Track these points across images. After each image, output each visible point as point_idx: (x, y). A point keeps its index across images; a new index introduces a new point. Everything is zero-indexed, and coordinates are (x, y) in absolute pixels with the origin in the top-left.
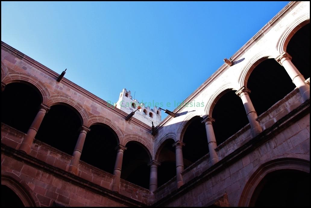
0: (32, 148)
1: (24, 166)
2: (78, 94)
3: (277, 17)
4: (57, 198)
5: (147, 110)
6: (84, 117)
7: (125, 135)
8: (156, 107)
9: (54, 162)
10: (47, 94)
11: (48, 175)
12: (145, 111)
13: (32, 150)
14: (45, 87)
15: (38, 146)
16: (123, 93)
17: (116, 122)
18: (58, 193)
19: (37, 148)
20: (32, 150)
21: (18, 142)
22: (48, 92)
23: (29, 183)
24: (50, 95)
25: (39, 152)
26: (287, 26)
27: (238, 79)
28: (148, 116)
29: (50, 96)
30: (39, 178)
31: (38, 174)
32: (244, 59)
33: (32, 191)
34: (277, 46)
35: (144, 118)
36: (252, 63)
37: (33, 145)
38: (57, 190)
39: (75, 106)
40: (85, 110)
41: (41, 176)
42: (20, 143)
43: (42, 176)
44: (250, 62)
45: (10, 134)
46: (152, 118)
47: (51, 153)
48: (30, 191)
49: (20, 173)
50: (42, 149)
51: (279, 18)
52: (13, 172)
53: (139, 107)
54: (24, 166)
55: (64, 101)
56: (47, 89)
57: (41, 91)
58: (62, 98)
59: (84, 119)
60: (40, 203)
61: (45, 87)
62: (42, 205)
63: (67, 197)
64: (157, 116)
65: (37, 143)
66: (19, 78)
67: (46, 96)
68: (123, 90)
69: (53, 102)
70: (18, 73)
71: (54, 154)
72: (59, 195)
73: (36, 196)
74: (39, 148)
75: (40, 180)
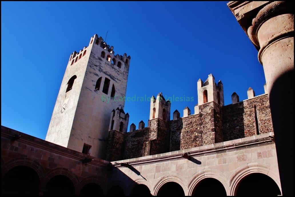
2: (35, 148)
3: (244, 144)
5: (116, 59)
7: (80, 181)
8: (126, 54)
12: (114, 60)
16: (93, 39)
17: (73, 170)
26: (249, 165)
27: (189, 184)
28: (116, 67)
32: (199, 163)
34: (231, 181)
35: (112, 69)
36: (205, 176)
39: (32, 166)
44: (204, 174)
46: (120, 68)
51: (245, 146)
53: (108, 55)
58: (17, 161)
64: (125, 65)
68: (95, 36)
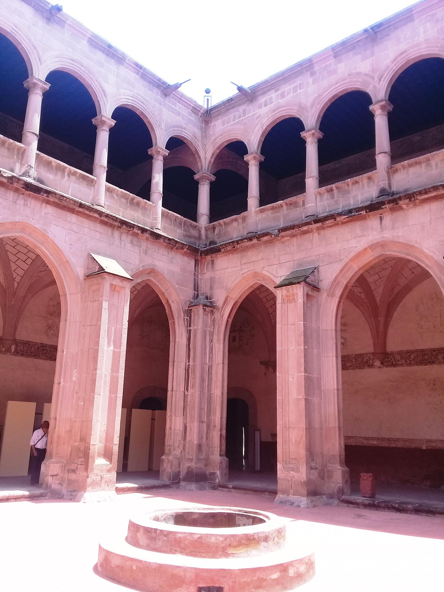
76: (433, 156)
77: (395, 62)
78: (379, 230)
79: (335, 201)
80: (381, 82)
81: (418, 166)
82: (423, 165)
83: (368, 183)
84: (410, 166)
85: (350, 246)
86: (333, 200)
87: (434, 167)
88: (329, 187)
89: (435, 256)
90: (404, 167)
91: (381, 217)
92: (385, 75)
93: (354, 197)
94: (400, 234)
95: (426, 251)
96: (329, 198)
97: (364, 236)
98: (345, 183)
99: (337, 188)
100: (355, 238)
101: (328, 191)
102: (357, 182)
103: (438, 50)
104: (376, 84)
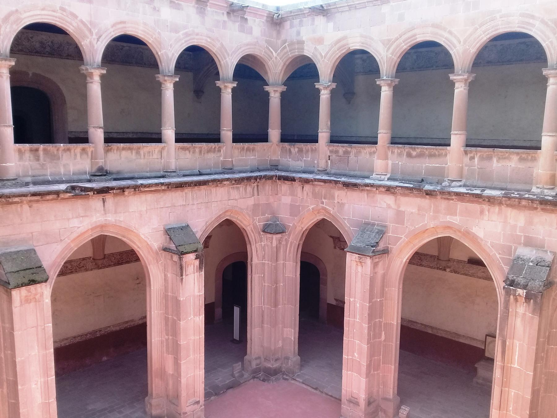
0: (466, 166)
1: (459, 206)
4: (522, 242)
6: (545, 42)
9: (509, 175)
10: (455, 41)
11: (497, 209)
13: (467, 168)
14: (444, 29)
15: (472, 158)
18: (522, 234)
19: (475, 161)
20: (467, 168)
21: (444, 165)
22: (455, 37)
23: (474, 228)
24: (460, 42)
25: (478, 168)
29: (462, 42)
30: (486, 218)
31: (482, 212)
33: (482, 240)
37: (466, 159)
38: (518, 228)
39: (519, 27)
40: (543, 22)
41: (487, 213)
42: (446, 166)
43: (489, 213)
45: (431, 156)
47: (499, 158)
48: (479, 240)
49: (458, 218)
50: (482, 158)
52: (449, 218)
54: (460, 206)
55: (493, 32)
56: (450, 33)
57: (444, 42)
58: (484, 28)
59: (548, 47)
60: (497, 254)
61: (444, 29)
62: (502, 256)
63: (539, 237)
65: (470, 153)
66: (403, 46)
67: (455, 47)
69: (471, 52)
70: (397, 39)
71: (505, 158)
72: (525, 236)
73: (490, 246)
74: (476, 160)
75: (488, 220)
76: (143, 147)
77: (114, 28)
78: (103, 212)
79: (40, 164)
80: (99, 42)
81: (129, 151)
82: (134, 152)
83: (81, 154)
84: (123, 149)
85: (71, 226)
86: (38, 162)
87: (142, 156)
88: (35, 146)
89: (148, 241)
90: (118, 149)
91: (103, 199)
92: (103, 37)
93: (64, 166)
94: (122, 219)
95: (143, 237)
96: (32, 158)
97: (87, 216)
98: (56, 147)
99: (45, 150)
100: (77, 217)
101: (31, 150)
102: (69, 150)
103: (152, 41)
104: (95, 42)
